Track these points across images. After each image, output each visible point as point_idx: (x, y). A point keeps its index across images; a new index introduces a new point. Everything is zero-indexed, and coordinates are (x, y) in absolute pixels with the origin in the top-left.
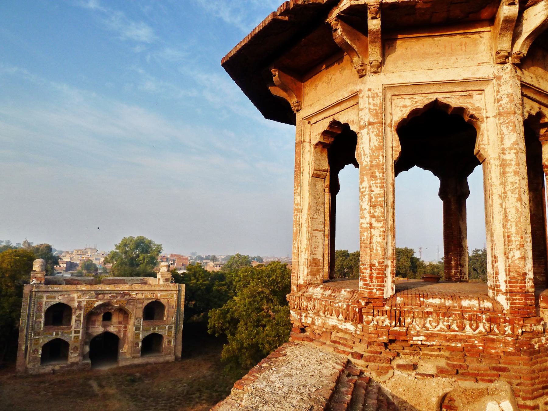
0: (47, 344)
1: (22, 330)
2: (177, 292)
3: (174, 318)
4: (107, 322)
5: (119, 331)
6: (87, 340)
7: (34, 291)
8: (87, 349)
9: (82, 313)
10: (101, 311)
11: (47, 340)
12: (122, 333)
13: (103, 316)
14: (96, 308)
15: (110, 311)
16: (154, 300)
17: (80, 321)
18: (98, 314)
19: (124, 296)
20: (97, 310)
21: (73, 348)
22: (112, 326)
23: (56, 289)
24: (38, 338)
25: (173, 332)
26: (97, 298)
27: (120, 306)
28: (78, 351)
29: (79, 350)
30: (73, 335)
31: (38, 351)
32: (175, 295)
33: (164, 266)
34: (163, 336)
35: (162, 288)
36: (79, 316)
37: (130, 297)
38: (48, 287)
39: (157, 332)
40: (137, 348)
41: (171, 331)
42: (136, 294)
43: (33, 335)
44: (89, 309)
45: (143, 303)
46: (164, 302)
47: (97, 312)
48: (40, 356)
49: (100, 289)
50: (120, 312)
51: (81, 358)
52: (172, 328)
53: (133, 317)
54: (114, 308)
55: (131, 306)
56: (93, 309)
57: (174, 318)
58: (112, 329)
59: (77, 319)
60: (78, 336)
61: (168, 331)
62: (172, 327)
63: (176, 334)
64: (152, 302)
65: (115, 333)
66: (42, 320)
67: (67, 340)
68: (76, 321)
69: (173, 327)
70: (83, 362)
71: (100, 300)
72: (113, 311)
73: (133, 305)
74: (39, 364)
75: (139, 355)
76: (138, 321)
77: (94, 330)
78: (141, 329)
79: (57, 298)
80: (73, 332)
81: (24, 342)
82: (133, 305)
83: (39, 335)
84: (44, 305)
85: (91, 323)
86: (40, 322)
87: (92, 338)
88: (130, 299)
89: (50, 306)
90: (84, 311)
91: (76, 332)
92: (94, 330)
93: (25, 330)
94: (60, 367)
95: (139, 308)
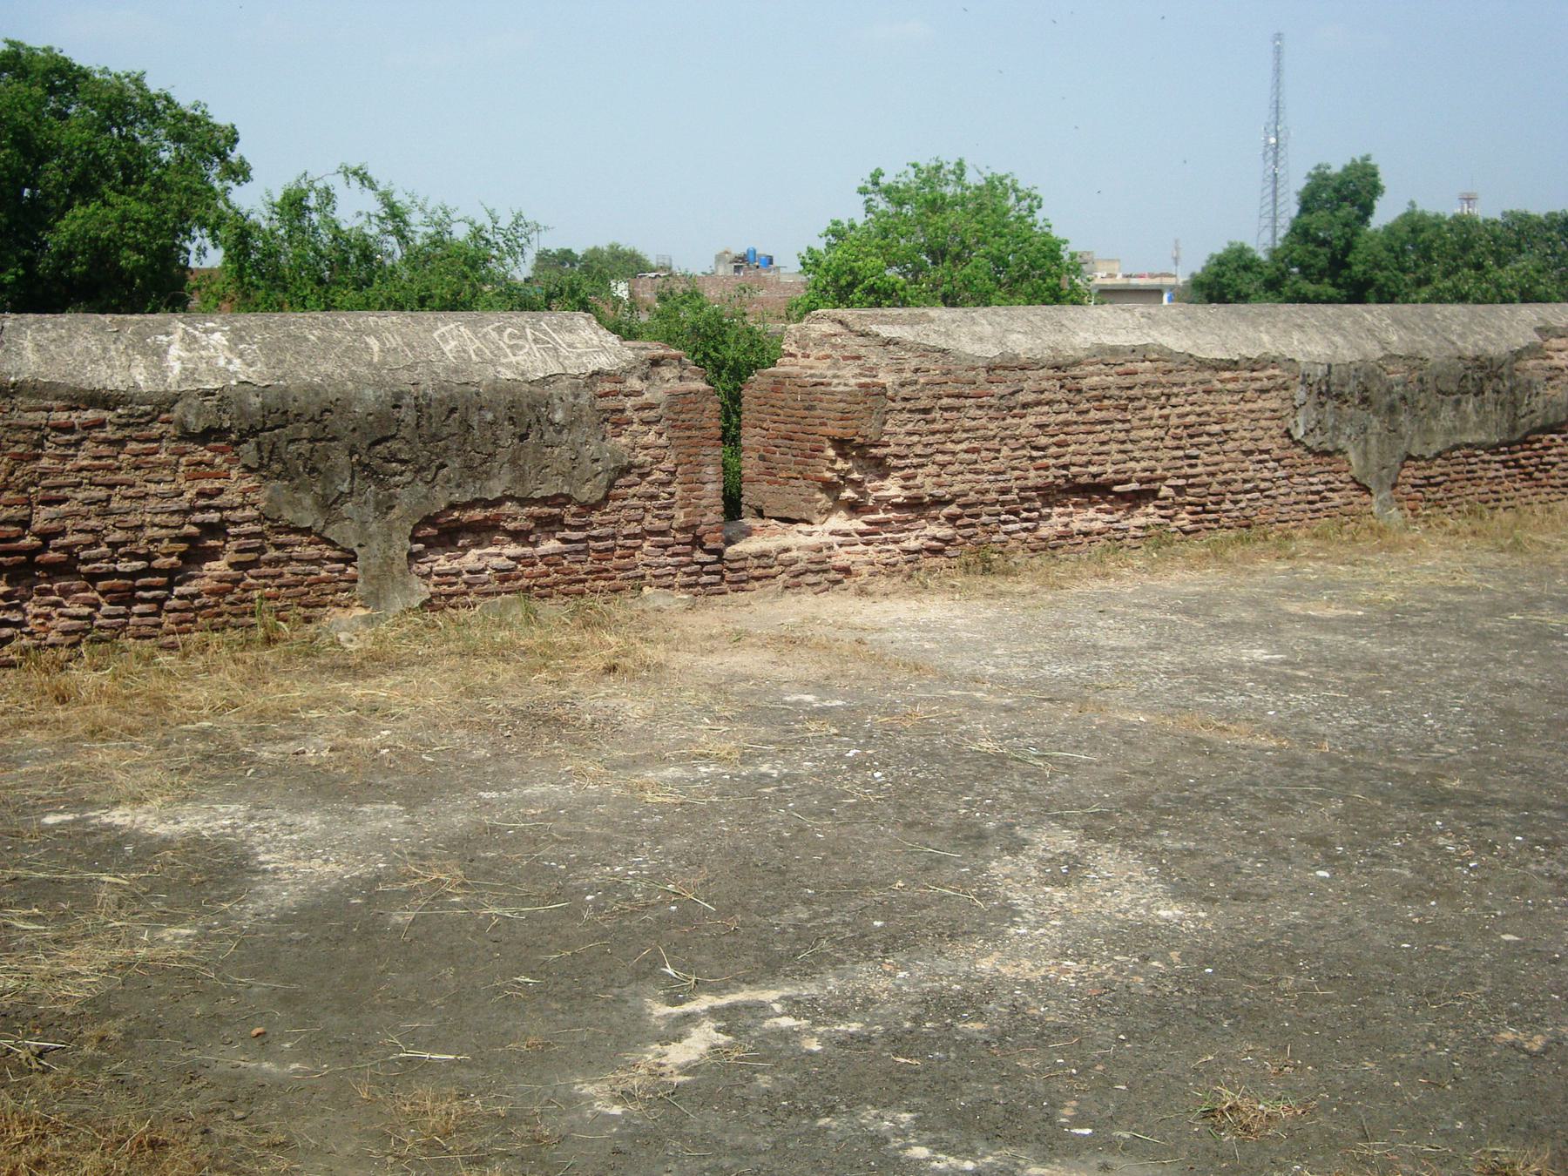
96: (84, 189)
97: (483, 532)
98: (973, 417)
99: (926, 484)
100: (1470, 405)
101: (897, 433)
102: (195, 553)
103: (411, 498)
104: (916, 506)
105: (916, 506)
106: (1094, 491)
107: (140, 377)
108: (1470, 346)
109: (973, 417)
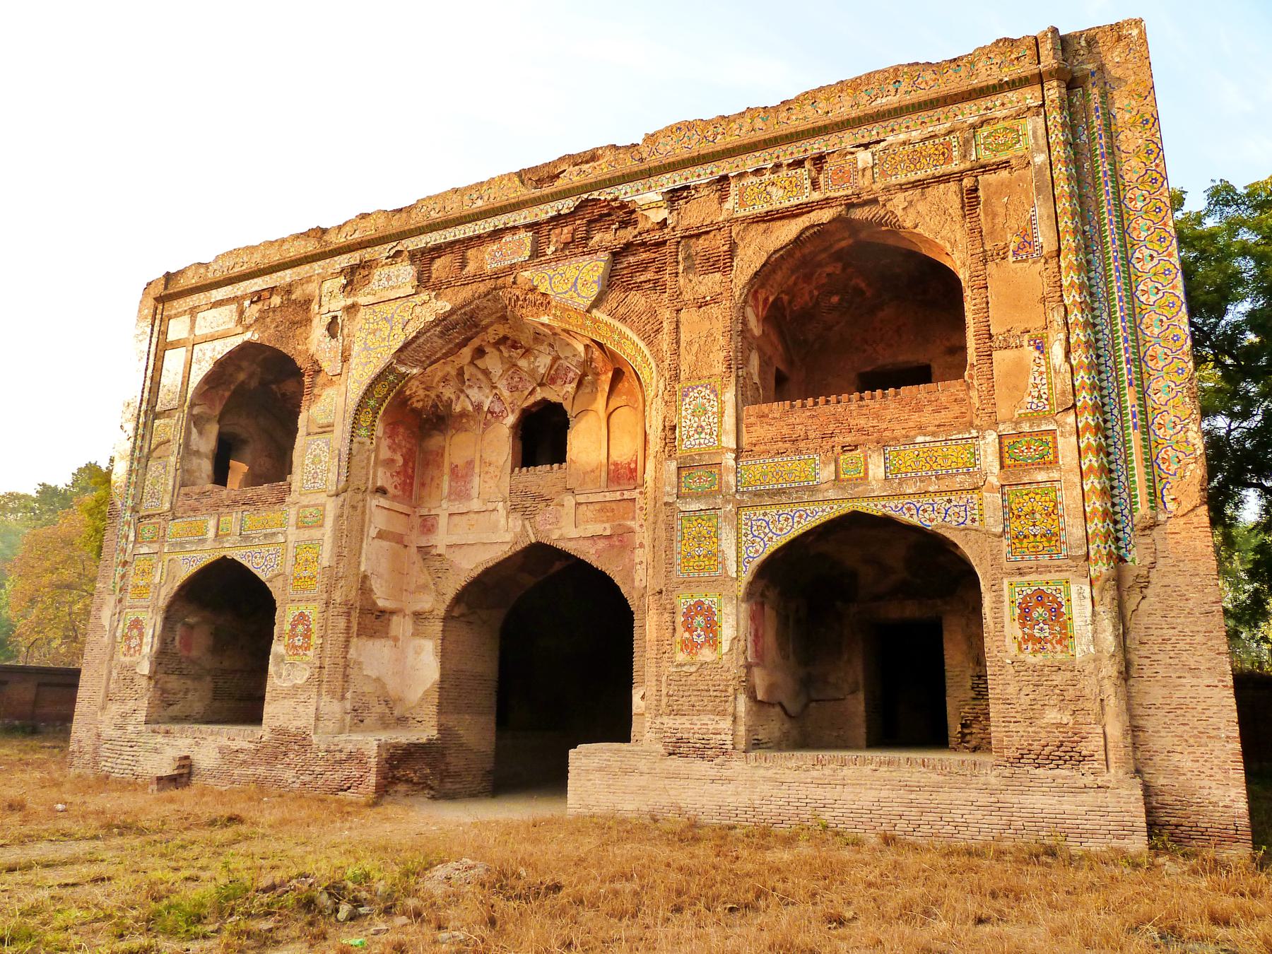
4: (542, 477)
10: (498, 398)
15: (553, 398)
16: (825, 215)
20: (475, 394)
28: (311, 653)
29: (315, 640)
30: (293, 534)
37: (628, 234)
39: (889, 508)
40: (706, 655)
47: (478, 407)
65: (591, 554)
69: (1066, 446)
73: (657, 285)
88: (628, 248)
95: (701, 304)
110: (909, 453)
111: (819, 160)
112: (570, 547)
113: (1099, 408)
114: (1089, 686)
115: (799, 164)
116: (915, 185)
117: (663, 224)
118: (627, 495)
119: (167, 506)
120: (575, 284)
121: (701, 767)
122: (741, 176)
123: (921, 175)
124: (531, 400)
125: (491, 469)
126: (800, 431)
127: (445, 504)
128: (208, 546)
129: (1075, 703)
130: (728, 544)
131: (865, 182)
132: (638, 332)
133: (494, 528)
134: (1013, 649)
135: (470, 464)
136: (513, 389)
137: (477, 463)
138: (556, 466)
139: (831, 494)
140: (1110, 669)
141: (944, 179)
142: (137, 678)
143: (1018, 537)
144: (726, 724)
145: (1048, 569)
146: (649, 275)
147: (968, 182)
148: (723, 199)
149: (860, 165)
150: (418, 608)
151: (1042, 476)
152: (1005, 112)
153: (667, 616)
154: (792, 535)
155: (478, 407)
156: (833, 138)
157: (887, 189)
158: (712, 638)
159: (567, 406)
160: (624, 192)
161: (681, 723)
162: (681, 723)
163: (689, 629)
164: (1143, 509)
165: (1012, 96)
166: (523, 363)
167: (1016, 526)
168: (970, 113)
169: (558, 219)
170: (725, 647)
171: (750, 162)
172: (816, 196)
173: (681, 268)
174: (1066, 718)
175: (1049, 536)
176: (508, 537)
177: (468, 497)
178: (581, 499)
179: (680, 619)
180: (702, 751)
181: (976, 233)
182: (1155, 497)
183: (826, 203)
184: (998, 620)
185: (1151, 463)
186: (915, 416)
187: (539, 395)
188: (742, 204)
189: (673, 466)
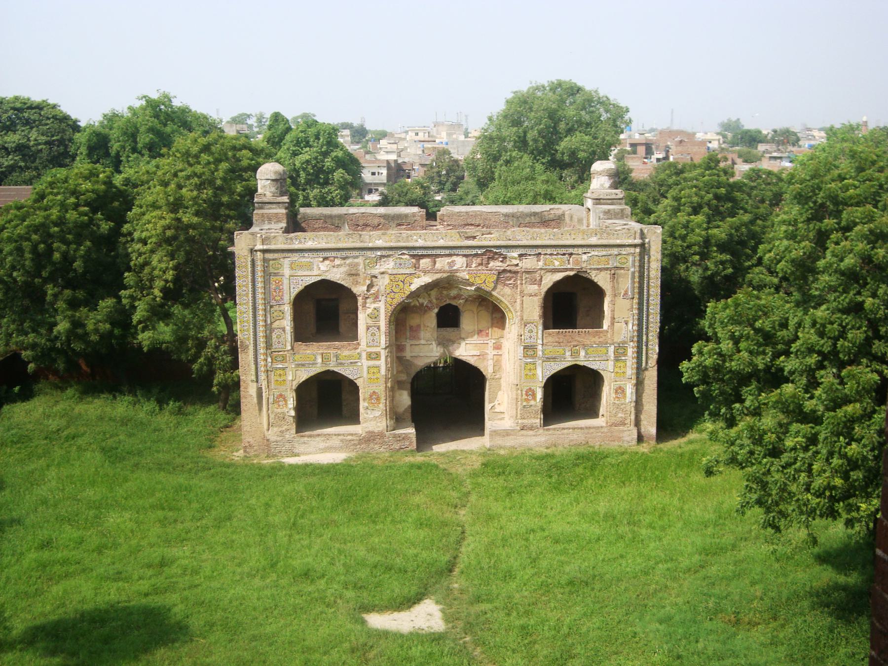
0: (303, 382)
1: (247, 347)
2: (638, 250)
3: (630, 325)
4: (449, 332)
5: (482, 356)
6: (403, 377)
7: (260, 251)
8: (405, 399)
9: (381, 305)
10: (430, 302)
11: (304, 375)
12: (491, 362)
13: (439, 315)
14: (415, 295)
15: (454, 304)
16: (572, 273)
17: (379, 328)
18: (422, 310)
19: (489, 264)
20: (421, 300)
21: (367, 396)
22: (463, 344)
23: (310, 244)
24: (283, 369)
25: (629, 363)
26: (416, 267)
27: (478, 289)
30: (365, 363)
31: (285, 400)
32: (631, 258)
33: (599, 173)
34: (602, 372)
35: (594, 240)
36: (374, 316)
38: (291, 239)
40: (532, 403)
41: (625, 361)
42: (521, 256)
43: (269, 360)
44: (399, 298)
45: (541, 280)
46: (602, 280)
47: (422, 304)
48: (293, 413)
49: (421, 243)
50: (480, 304)
51: (391, 423)
52: (624, 354)
53: (517, 320)
54: (465, 295)
55: (507, 290)
56: (408, 297)
57: (630, 325)
58: (466, 351)
59: (370, 322)
60: (378, 367)
61: (617, 359)
62: (625, 349)
63: (640, 370)
64: (566, 279)
65: (472, 361)
66: (287, 323)
67: (350, 377)
68: (368, 329)
70: (398, 432)
71: (425, 272)
72: (461, 301)
73: (515, 286)
74: (294, 431)
75: (538, 420)
76: (531, 331)
77: (416, 351)
78: (540, 353)
79: (315, 267)
80: (364, 355)
81: (254, 378)
82: (515, 286)
83: (284, 359)
84: (285, 287)
85: (408, 334)
86: (284, 329)
87: (413, 374)
88: (504, 271)
89: (301, 288)
90: (386, 302)
91: (370, 356)
92: (416, 351)
93: (251, 348)
94: (342, 441)
95: (531, 295)
96: (570, 131)
97: (403, 225)
98: (455, 217)
99: (449, 223)
100: (533, 217)
101: (445, 218)
102: (379, 225)
103: (396, 222)
104: (448, 225)
105: (448, 225)
106: (472, 225)
107: (375, 212)
108: (533, 211)
109: (455, 217)
110: (592, 349)
111: (571, 254)
112: (464, 358)
113: (638, 342)
114: (628, 408)
115: (564, 254)
116: (598, 269)
117: (517, 265)
118: (485, 342)
119: (289, 348)
120: (485, 281)
121: (531, 433)
122: (546, 254)
123: (600, 267)
124: (445, 303)
125: (428, 329)
126: (561, 340)
127: (408, 341)
128: (319, 365)
129: (625, 412)
130: (539, 372)
131: (584, 265)
132: (509, 302)
133: (432, 351)
134: (612, 399)
135: (419, 326)
136: (437, 299)
137: (422, 326)
138: (456, 329)
139: (570, 359)
140: (633, 404)
141: (607, 269)
142: (286, 417)
143: (617, 373)
144: (538, 421)
145: (622, 381)
146: (511, 282)
147: (613, 272)
148: (539, 260)
149: (583, 260)
150: (400, 379)
151: (623, 358)
152: (624, 253)
153: (519, 392)
154: (558, 369)
155: (422, 304)
156: (576, 249)
157: (590, 269)
158: (534, 398)
159: (460, 307)
160: (504, 251)
161: (524, 421)
162: (525, 421)
163: (527, 395)
164: (644, 365)
165: (628, 249)
166: (445, 292)
167: (616, 370)
168: (615, 251)
169: (476, 255)
170: (538, 400)
171: (549, 251)
172: (569, 267)
173: (524, 282)
174: (623, 416)
175: (624, 372)
176: (438, 354)
177: (419, 339)
178: (467, 342)
179: (524, 393)
180: (531, 428)
181: (613, 287)
182: (647, 363)
183: (572, 269)
184: (610, 393)
185: (647, 354)
186: (593, 339)
187: (448, 302)
188: (545, 264)
189: (522, 348)
